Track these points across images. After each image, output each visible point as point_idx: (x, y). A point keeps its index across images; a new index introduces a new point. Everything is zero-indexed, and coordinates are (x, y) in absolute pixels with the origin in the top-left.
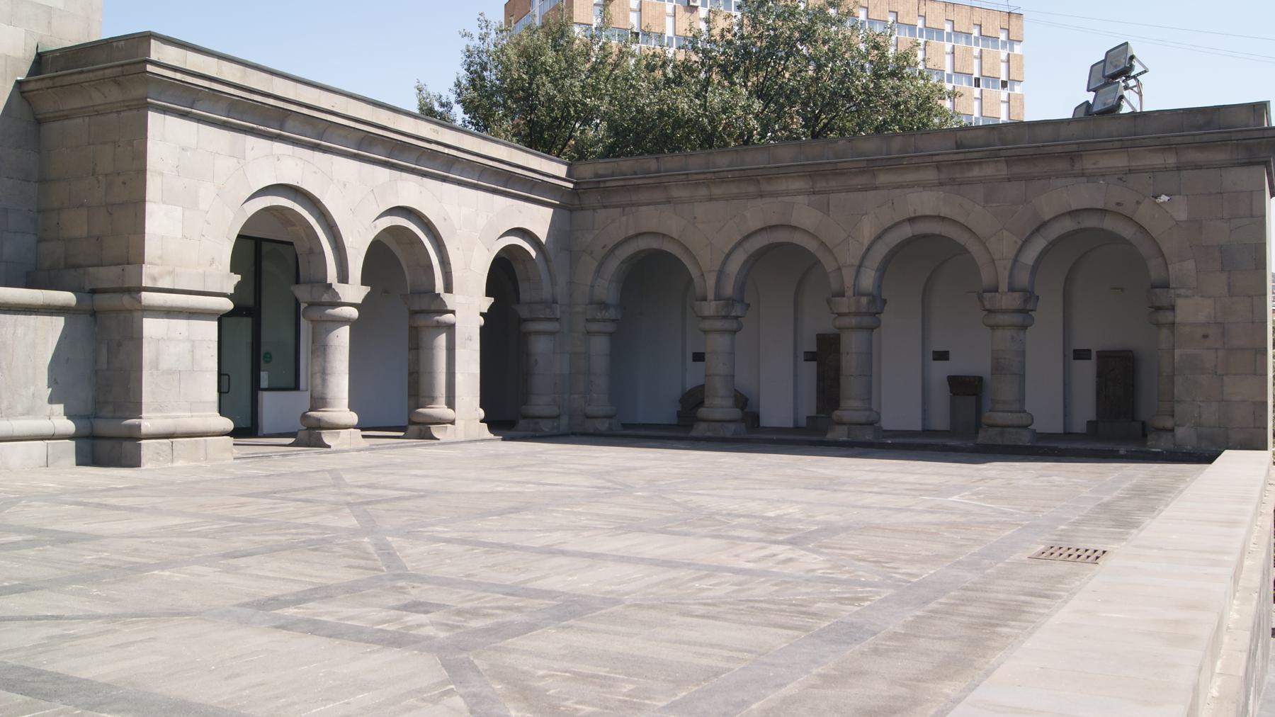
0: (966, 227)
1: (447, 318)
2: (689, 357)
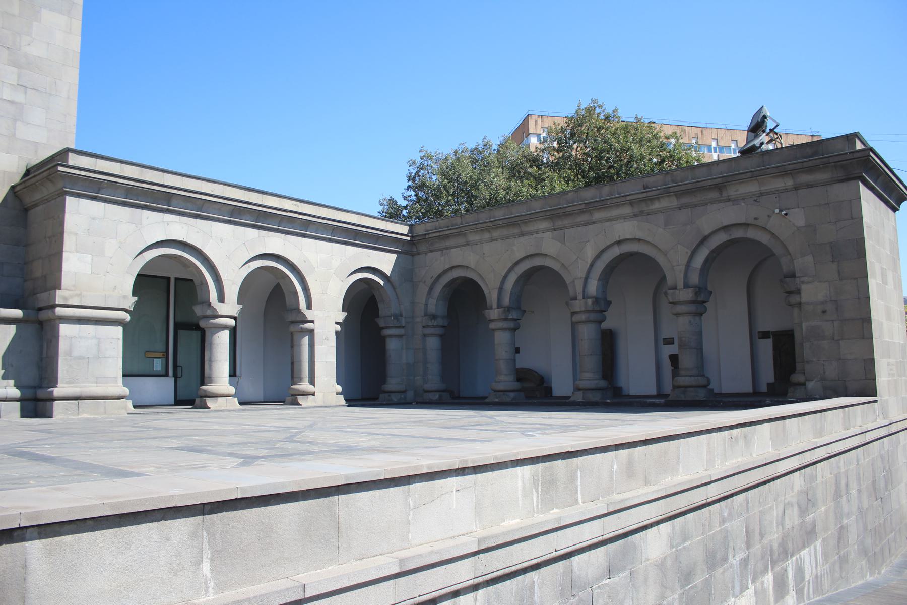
0: (653, 244)
1: (309, 325)
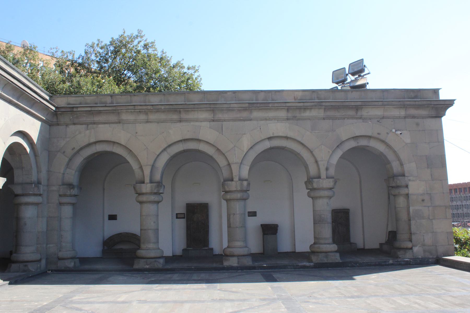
2: (106, 218)
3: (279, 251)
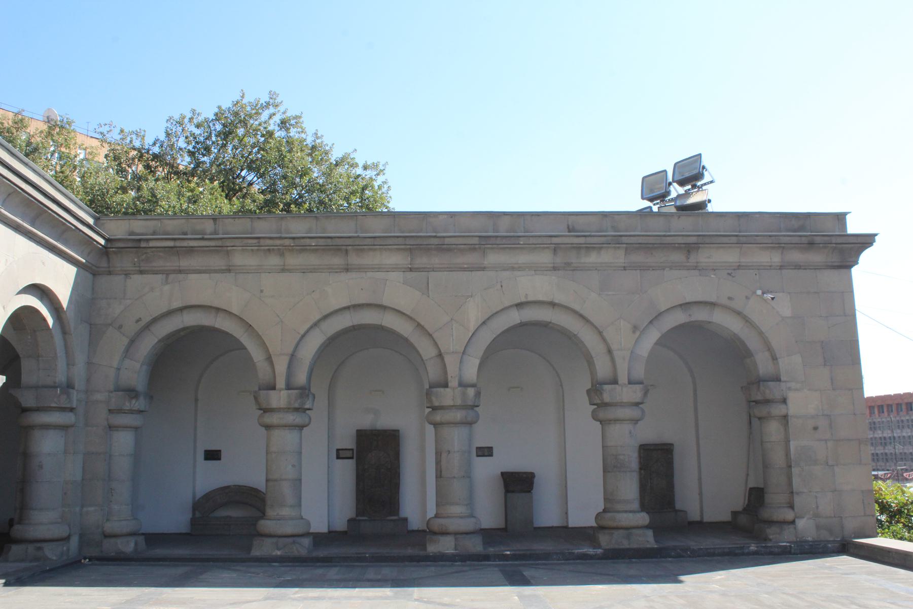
2: (200, 456)
3: (537, 524)
